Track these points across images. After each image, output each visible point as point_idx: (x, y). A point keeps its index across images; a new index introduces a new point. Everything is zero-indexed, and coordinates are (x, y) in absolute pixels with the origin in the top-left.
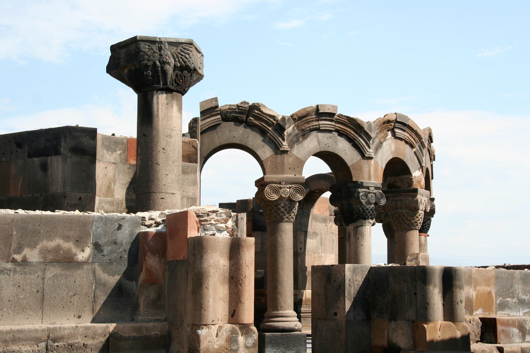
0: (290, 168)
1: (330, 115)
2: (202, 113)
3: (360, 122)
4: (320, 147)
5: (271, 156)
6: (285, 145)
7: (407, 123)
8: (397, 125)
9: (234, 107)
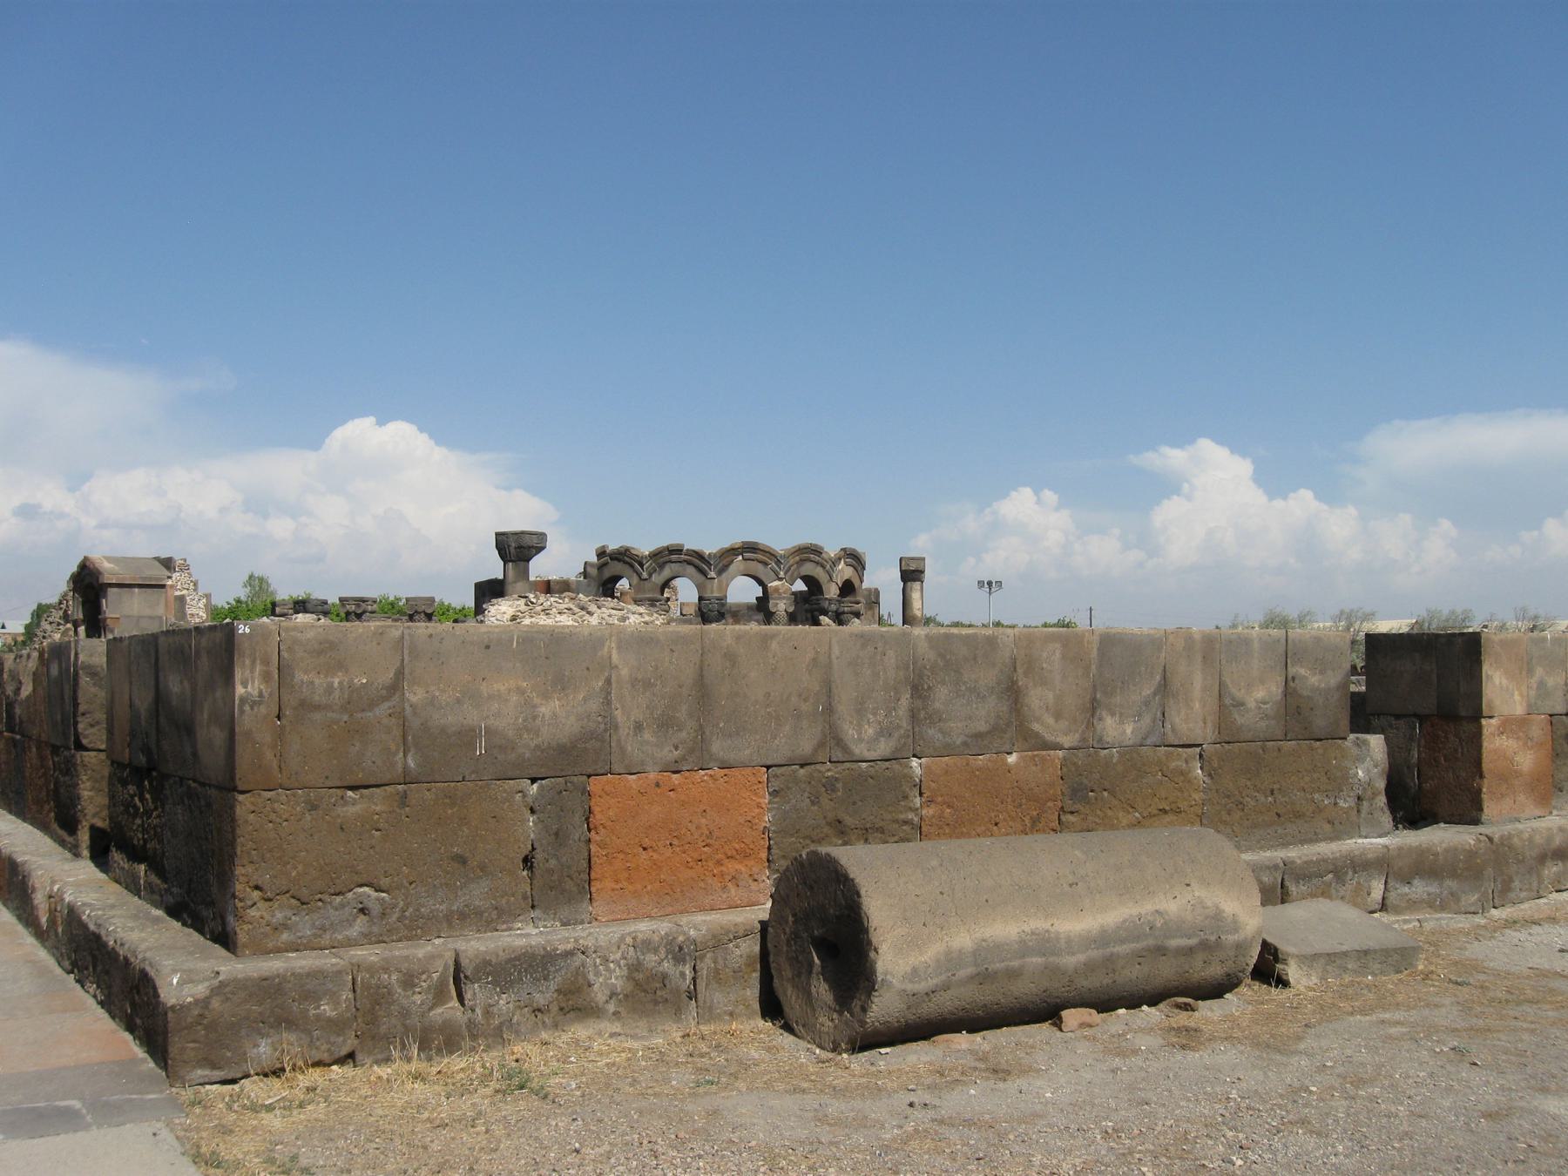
2: (598, 556)
6: (645, 575)
8: (744, 550)
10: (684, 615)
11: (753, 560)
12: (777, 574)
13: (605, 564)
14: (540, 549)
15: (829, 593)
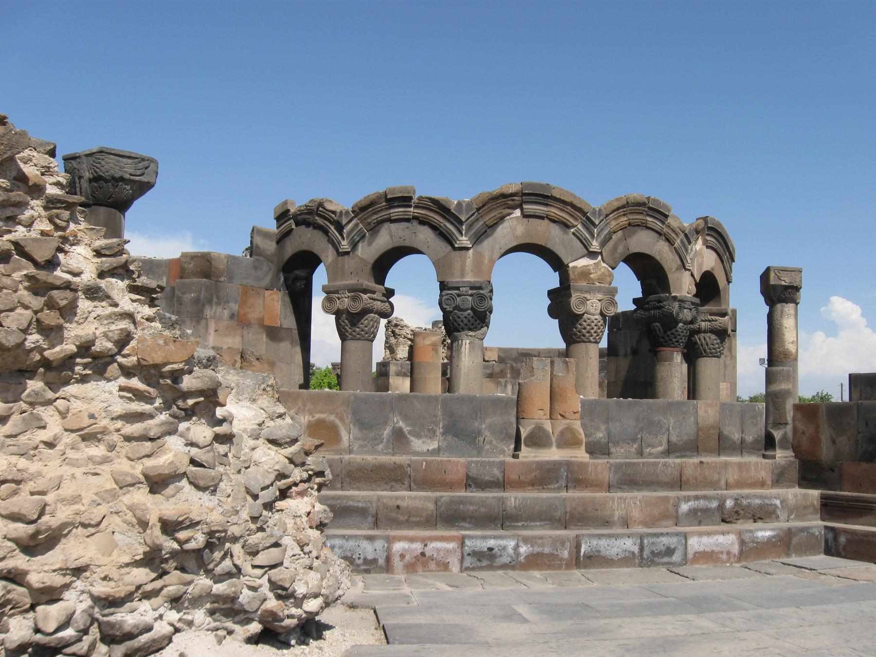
0: (351, 273)
1: (405, 200)
3: (446, 201)
4: (393, 242)
5: (333, 261)
6: (345, 245)
7: (549, 193)
9: (303, 209)
10: (487, 361)
11: (542, 218)
12: (585, 245)
13: (288, 233)
14: (144, 187)
15: (680, 289)
